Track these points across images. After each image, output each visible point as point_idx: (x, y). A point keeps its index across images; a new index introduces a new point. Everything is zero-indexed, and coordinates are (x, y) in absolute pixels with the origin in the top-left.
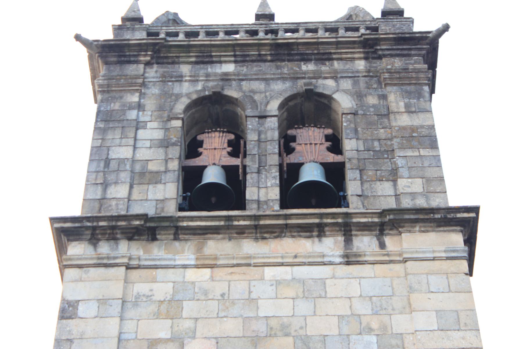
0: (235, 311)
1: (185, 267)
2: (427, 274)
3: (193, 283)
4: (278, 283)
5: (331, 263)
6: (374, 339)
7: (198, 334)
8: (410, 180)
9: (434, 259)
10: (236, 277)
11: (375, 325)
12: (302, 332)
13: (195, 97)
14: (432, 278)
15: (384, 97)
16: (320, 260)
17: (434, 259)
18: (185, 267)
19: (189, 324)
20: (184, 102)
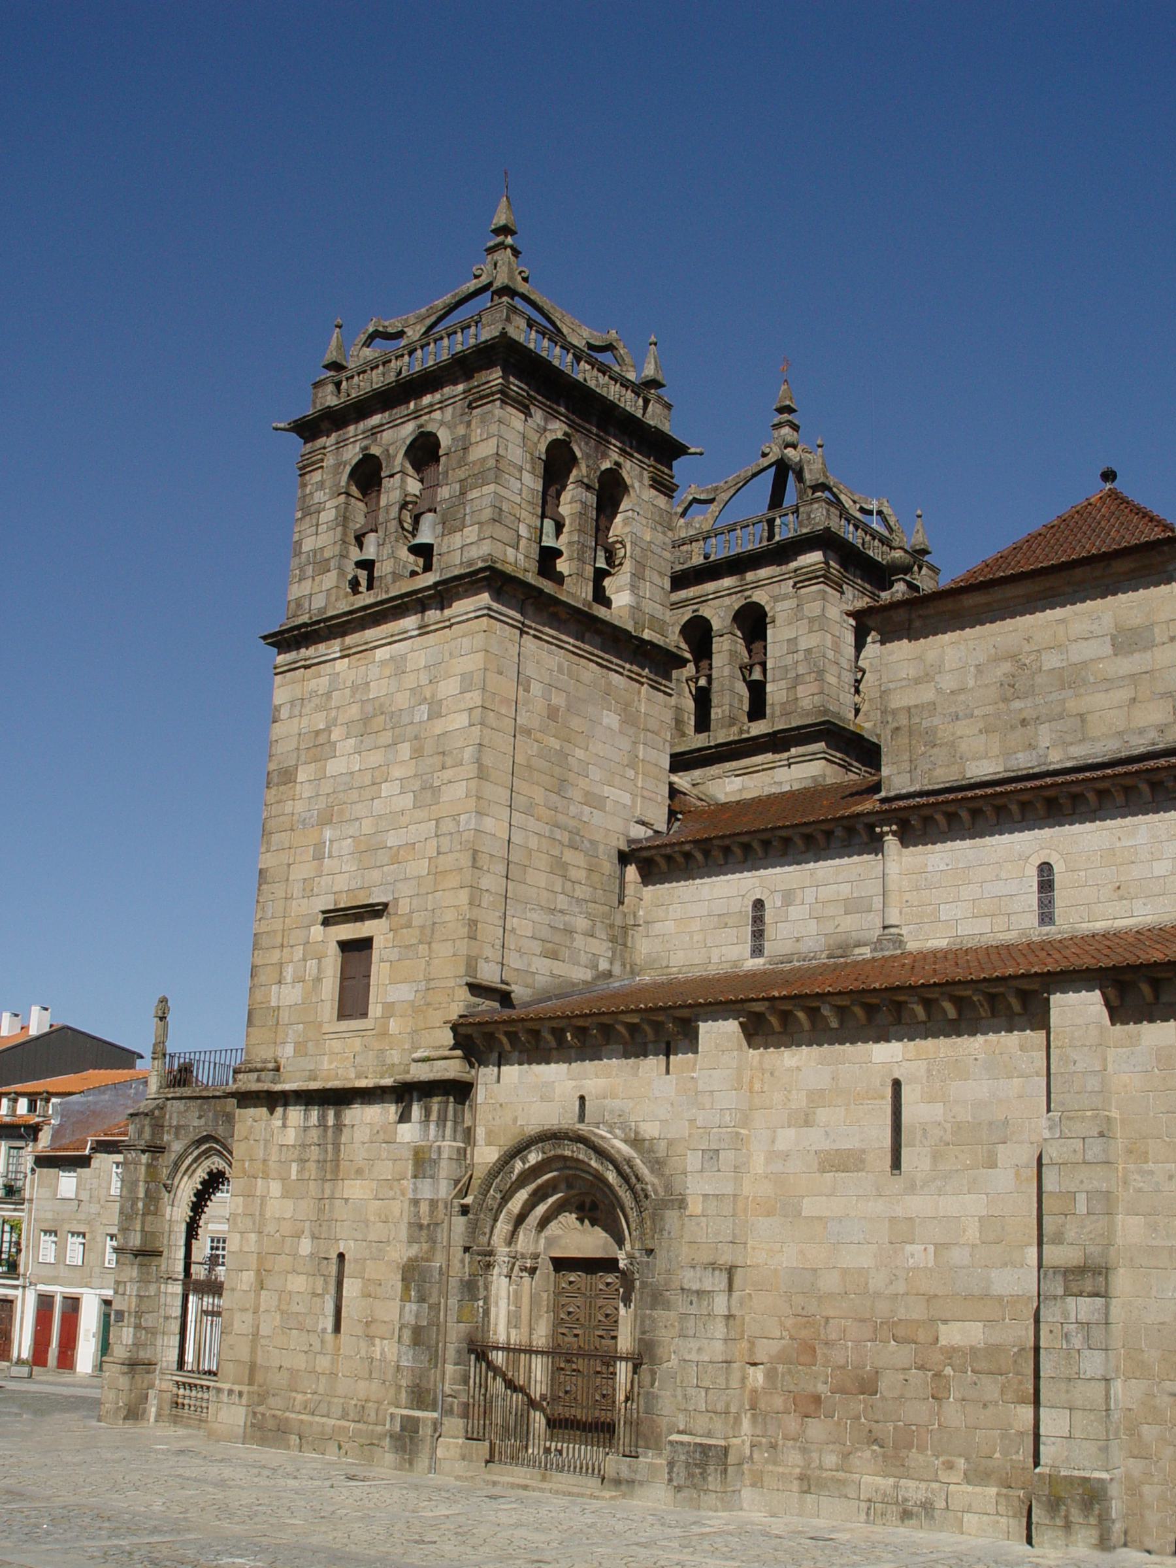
0: (358, 696)
1: (334, 659)
2: (462, 636)
3: (338, 674)
4: (383, 663)
5: (411, 637)
6: (427, 706)
7: (339, 722)
8: (470, 528)
9: (468, 620)
10: (363, 662)
11: (428, 696)
12: (390, 709)
13: (354, 462)
14: (464, 639)
15: (469, 424)
16: (405, 636)
17: (468, 620)
18: (334, 659)
19: (334, 713)
20: (348, 469)
